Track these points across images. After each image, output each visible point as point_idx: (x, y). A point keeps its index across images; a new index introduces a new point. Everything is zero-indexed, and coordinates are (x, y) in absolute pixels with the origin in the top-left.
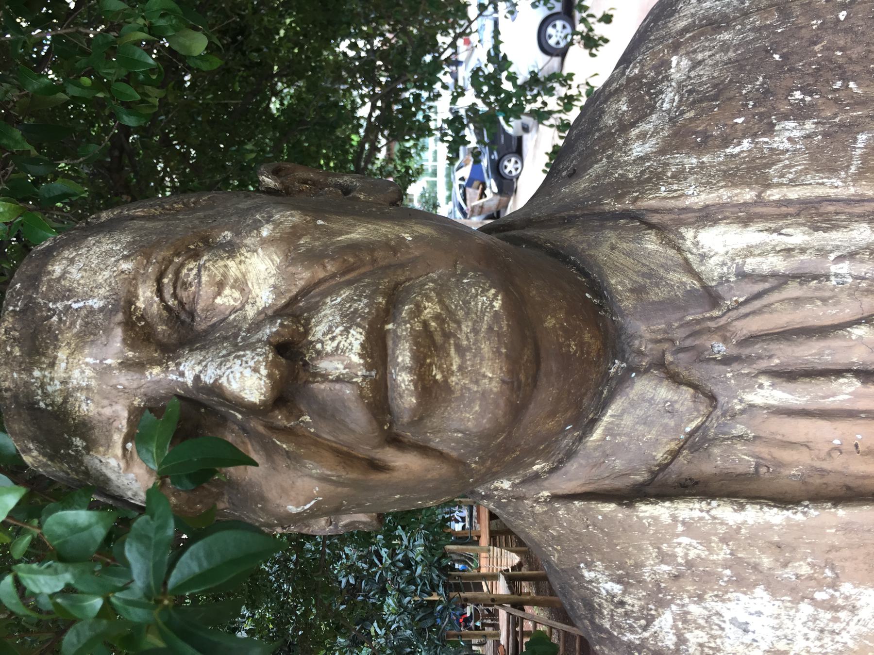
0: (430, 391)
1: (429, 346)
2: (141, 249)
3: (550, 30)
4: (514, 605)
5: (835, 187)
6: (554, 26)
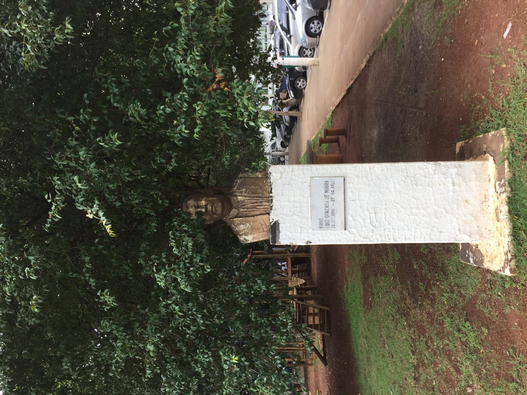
0: (215, 210)
1: (216, 207)
2: (195, 201)
3: (312, 25)
4: (299, 299)
5: (246, 194)
6: (313, 23)
